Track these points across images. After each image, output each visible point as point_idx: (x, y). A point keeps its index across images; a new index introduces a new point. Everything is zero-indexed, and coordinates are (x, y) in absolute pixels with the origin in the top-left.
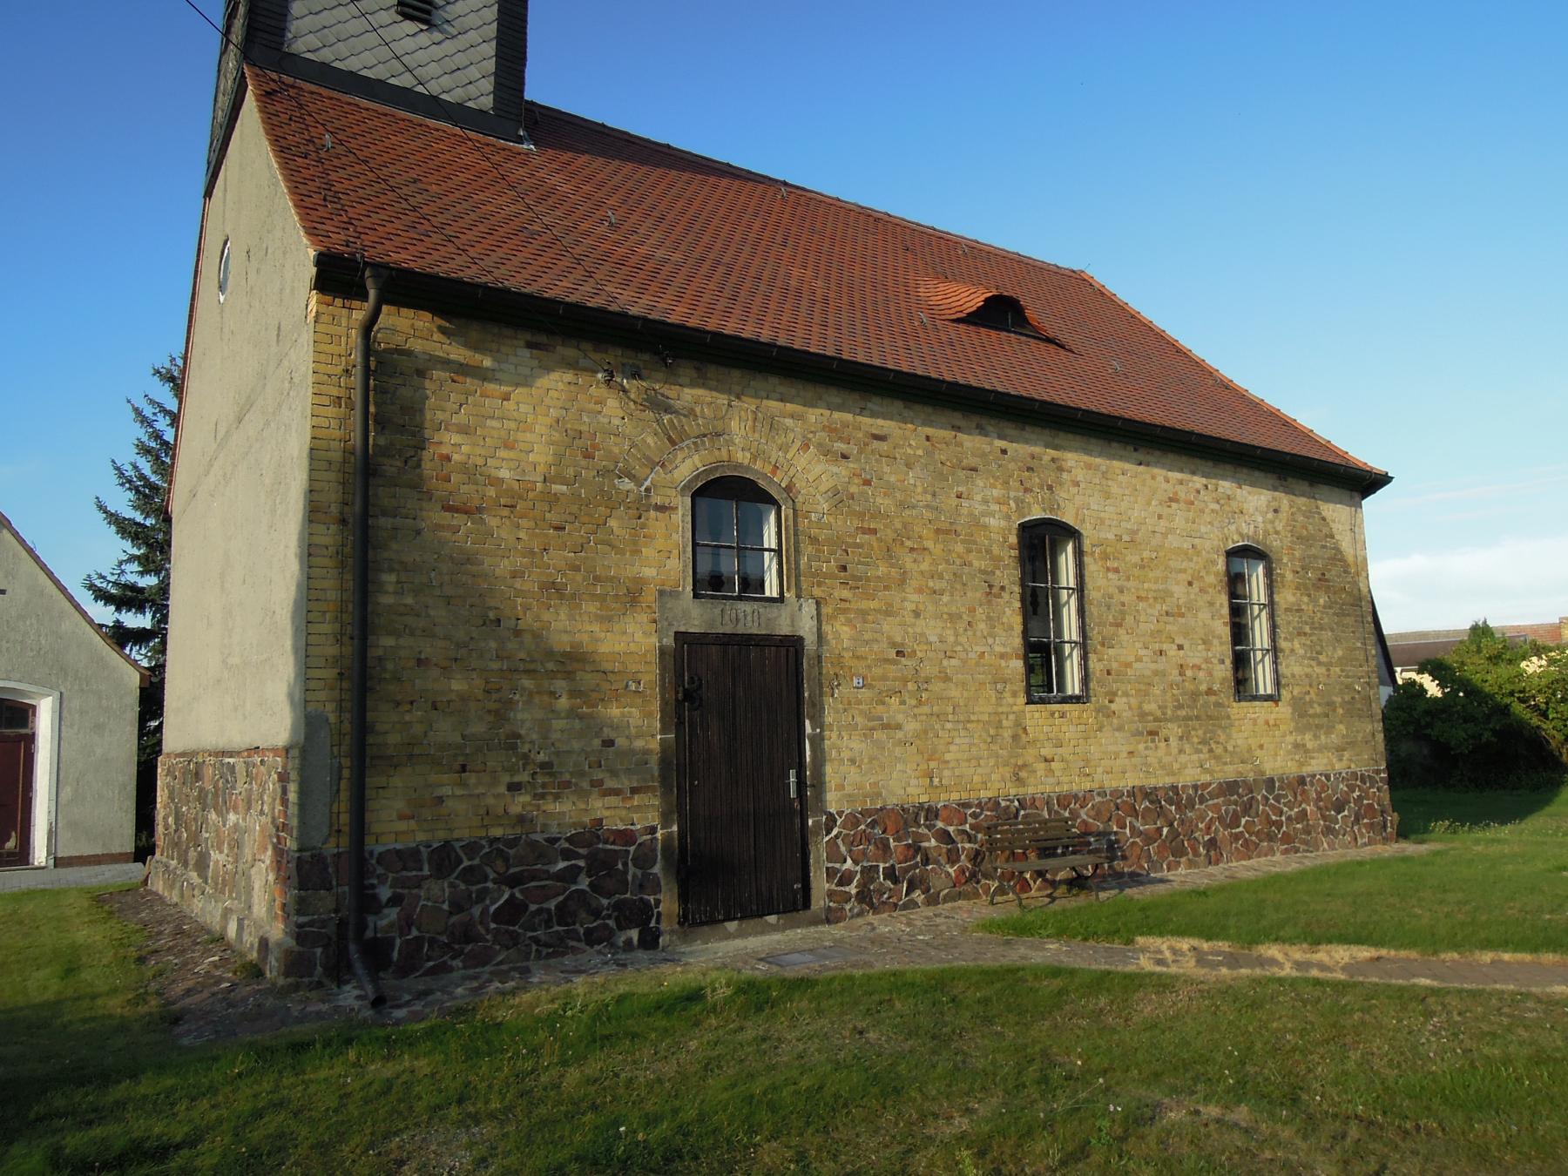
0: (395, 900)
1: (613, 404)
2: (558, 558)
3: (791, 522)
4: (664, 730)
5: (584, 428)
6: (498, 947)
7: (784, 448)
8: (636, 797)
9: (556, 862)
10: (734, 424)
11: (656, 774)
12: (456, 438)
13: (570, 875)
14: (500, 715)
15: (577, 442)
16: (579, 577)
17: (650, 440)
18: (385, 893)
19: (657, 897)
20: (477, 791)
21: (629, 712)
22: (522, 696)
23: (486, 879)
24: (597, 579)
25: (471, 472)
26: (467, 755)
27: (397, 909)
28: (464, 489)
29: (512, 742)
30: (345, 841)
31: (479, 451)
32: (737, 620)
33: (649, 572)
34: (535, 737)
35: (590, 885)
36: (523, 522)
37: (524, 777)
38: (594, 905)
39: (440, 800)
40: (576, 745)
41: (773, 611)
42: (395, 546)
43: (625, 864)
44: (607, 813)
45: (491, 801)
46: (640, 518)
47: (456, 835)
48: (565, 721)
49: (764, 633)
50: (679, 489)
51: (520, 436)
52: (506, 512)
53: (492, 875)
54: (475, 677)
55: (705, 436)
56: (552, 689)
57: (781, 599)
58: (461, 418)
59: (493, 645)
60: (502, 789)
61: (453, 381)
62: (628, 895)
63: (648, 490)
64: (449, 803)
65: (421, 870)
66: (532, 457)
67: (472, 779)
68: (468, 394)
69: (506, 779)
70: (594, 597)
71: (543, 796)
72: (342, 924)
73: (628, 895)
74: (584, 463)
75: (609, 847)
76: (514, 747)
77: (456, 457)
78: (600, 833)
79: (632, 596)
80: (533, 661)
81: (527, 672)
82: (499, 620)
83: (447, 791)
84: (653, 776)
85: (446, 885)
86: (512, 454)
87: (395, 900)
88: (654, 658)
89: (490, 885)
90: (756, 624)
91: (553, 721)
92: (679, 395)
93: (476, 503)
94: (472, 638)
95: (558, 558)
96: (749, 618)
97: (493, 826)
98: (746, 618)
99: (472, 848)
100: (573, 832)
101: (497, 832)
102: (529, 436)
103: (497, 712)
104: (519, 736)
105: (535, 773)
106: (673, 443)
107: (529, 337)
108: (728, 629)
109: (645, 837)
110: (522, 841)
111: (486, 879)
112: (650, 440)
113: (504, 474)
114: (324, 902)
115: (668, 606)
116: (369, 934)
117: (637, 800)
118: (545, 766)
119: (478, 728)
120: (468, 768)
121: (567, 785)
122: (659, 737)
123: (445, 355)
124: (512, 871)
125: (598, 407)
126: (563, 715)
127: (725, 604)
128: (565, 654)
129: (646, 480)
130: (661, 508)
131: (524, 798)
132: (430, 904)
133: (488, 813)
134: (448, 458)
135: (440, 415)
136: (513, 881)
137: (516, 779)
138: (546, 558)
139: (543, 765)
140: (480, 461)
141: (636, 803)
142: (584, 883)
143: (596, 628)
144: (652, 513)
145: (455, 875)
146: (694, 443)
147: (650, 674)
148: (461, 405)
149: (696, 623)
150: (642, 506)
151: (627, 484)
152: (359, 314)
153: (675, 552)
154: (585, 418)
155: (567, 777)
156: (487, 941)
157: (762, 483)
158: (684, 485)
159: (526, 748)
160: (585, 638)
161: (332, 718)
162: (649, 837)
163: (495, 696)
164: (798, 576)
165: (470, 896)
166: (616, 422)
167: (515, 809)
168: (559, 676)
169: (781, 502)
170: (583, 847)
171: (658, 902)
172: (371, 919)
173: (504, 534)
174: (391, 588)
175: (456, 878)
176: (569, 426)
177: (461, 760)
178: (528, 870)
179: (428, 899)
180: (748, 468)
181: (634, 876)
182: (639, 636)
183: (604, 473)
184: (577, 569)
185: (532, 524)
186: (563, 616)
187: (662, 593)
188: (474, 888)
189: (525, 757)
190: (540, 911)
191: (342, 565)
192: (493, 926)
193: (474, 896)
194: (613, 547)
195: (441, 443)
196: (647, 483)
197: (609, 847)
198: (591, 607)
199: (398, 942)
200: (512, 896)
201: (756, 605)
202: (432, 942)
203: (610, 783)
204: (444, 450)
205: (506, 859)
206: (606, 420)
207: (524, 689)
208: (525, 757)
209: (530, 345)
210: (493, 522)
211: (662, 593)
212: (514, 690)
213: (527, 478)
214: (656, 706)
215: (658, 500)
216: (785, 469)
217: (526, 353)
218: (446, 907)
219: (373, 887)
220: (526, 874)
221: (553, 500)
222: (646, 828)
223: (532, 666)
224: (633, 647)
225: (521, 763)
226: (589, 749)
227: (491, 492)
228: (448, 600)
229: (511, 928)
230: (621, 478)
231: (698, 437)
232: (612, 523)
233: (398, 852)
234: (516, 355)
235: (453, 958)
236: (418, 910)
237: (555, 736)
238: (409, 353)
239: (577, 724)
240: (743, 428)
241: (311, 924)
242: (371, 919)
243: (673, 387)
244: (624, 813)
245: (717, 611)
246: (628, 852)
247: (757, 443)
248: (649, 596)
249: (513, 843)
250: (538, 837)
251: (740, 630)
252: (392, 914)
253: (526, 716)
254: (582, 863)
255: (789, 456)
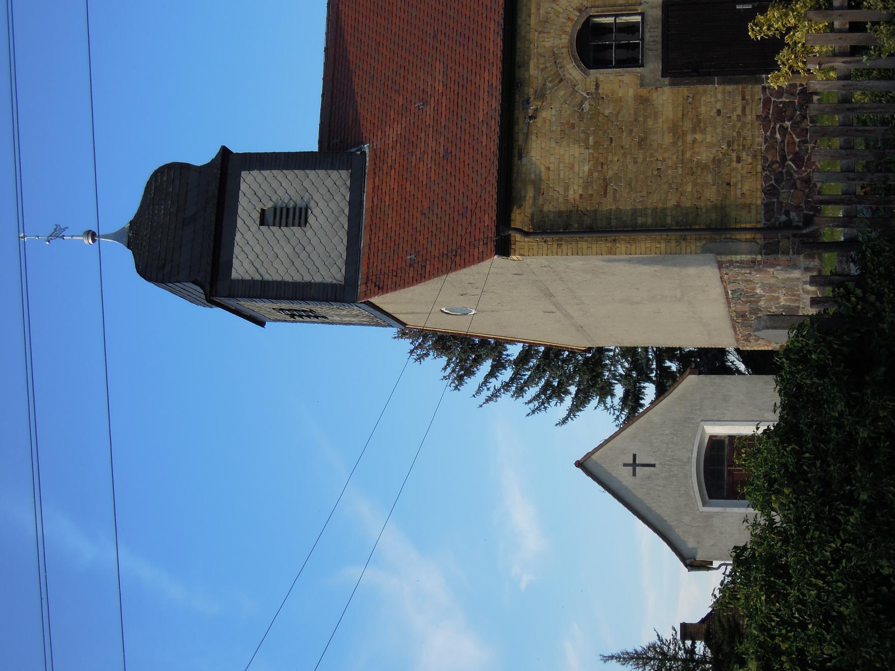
0: (787, 213)
1: (544, 114)
2: (626, 141)
3: (600, 9)
4: (713, 83)
5: (559, 129)
6: (814, 167)
7: (557, 13)
8: (747, 97)
9: (776, 138)
10: (547, 45)
11: (736, 86)
12: (571, 192)
13: (783, 130)
14: (705, 167)
15: (567, 131)
16: (636, 130)
17: (562, 93)
18: (783, 218)
19: (798, 86)
20: (740, 177)
21: (703, 102)
22: (694, 157)
23: (781, 172)
24: (636, 120)
25: (587, 184)
26: (722, 183)
27: (791, 212)
28: (595, 187)
29: (717, 162)
30: (758, 236)
31: (576, 181)
32: (654, 41)
33: (631, 92)
34: (714, 151)
35: (789, 121)
36: (610, 158)
37: (734, 156)
38: (799, 119)
39: (743, 194)
40: (719, 130)
41: (649, 19)
42: (625, 218)
43: (781, 102)
44: (754, 113)
45: (744, 171)
46: (603, 98)
47: (759, 187)
48: (707, 136)
49: (661, 25)
50: (586, 77)
51: (567, 161)
52: (605, 167)
53: (780, 169)
54: (685, 180)
55: (555, 62)
56: (691, 142)
57: (642, 14)
58: (561, 190)
59: (670, 172)
60: (739, 166)
61: (543, 194)
62: (796, 101)
63: (588, 94)
64: (744, 191)
65: (774, 202)
66: (577, 155)
67: (733, 180)
68: (549, 187)
69: (734, 164)
70: (645, 121)
71: (744, 146)
72: (795, 236)
73: (796, 101)
74: (577, 129)
75: (771, 111)
76: (719, 161)
77: (580, 192)
78: (763, 116)
79: (643, 101)
80: (678, 152)
81: (683, 154)
82: (658, 169)
83: (739, 192)
84: (736, 89)
85: (782, 191)
86: (576, 166)
87: (787, 213)
88: (676, 89)
89: (784, 170)
90: (656, 30)
91: (707, 141)
92: (535, 78)
93: (601, 181)
94: (667, 182)
95: (626, 141)
96: (653, 34)
97: (756, 170)
98: (653, 36)
99: (766, 179)
100: (762, 130)
101: (759, 168)
102: (567, 157)
103: (703, 169)
104: (714, 158)
105: (732, 150)
106: (561, 80)
107: (516, 158)
108: (659, 46)
109: (767, 93)
110: (765, 155)
111: (781, 172)
112: (562, 93)
113: (586, 168)
114: (784, 243)
115: (648, 82)
116: (801, 224)
117: (748, 97)
118: (729, 145)
119: (710, 178)
120: (728, 182)
121: (739, 133)
122: (716, 86)
123: (531, 199)
124: (778, 160)
125: (547, 122)
126: (704, 136)
127: (646, 49)
128: (674, 135)
129: (583, 95)
130: (597, 86)
131: (744, 155)
132: (790, 198)
133: (750, 173)
134: (581, 195)
135: (561, 200)
136: (784, 159)
137: (735, 159)
138: (626, 147)
139: (729, 145)
140: (581, 181)
141: (750, 98)
142: (788, 124)
143: (660, 121)
144: (600, 91)
145: (778, 187)
146: (561, 68)
147: (684, 90)
148: (555, 190)
149: (657, 66)
150: (597, 97)
151: (586, 106)
152: (518, 237)
153: (620, 78)
154: (554, 128)
155: (735, 134)
156: (810, 171)
157: (578, 27)
158: (584, 73)
159: (721, 155)
160: (666, 126)
161: (704, 242)
162: (767, 90)
163: (695, 170)
164: (630, 5)
165: (788, 180)
166: (554, 112)
167: (750, 160)
168: (685, 139)
169: (588, 16)
170: (770, 125)
171: (801, 85)
172: (794, 224)
173: (616, 168)
174: (644, 219)
175: (780, 186)
176: (559, 137)
177: (725, 185)
178: (779, 152)
179: (788, 199)
180: (571, 36)
181: (786, 98)
182: (665, 97)
183: (581, 118)
184: (631, 130)
185: (610, 154)
186: (655, 137)
187: (642, 85)
188: (785, 178)
189: (724, 155)
190: (799, 146)
191: (634, 240)
192: (803, 169)
193: (789, 178)
194: (619, 112)
195: (574, 199)
196: (584, 94)
197: (771, 111)
198: (650, 123)
199: (805, 212)
200: (791, 160)
201: (646, 30)
202: (807, 197)
203: (739, 112)
204: (577, 197)
205: (774, 162)
206: (554, 117)
207: (691, 156)
208: (724, 155)
209: (520, 158)
210: (610, 174)
211: (642, 85)
212: (692, 161)
213: (588, 157)
214: (700, 88)
215: (593, 91)
216: (569, 13)
217: (524, 159)
218: (792, 191)
219: (780, 223)
220: (781, 154)
221: (597, 144)
222: (763, 92)
223: (680, 152)
224: (670, 101)
225: (727, 157)
226: (722, 123)
227: (596, 174)
228: (649, 193)
229: (806, 160)
230: (583, 109)
231: (557, 67)
232: (607, 112)
233: (765, 213)
234: (526, 165)
235: (816, 187)
236: (792, 203)
237: (715, 140)
238: (532, 215)
239: (709, 129)
240: (549, 40)
241: (793, 249)
242: (794, 224)
243: (531, 81)
244: (754, 104)
245: (650, 53)
246: (774, 101)
247: (556, 31)
248: (644, 92)
249: (765, 159)
250: (763, 147)
251: (659, 39)
252: (793, 215)
253: (704, 155)
254: (778, 126)
255: (561, 11)
